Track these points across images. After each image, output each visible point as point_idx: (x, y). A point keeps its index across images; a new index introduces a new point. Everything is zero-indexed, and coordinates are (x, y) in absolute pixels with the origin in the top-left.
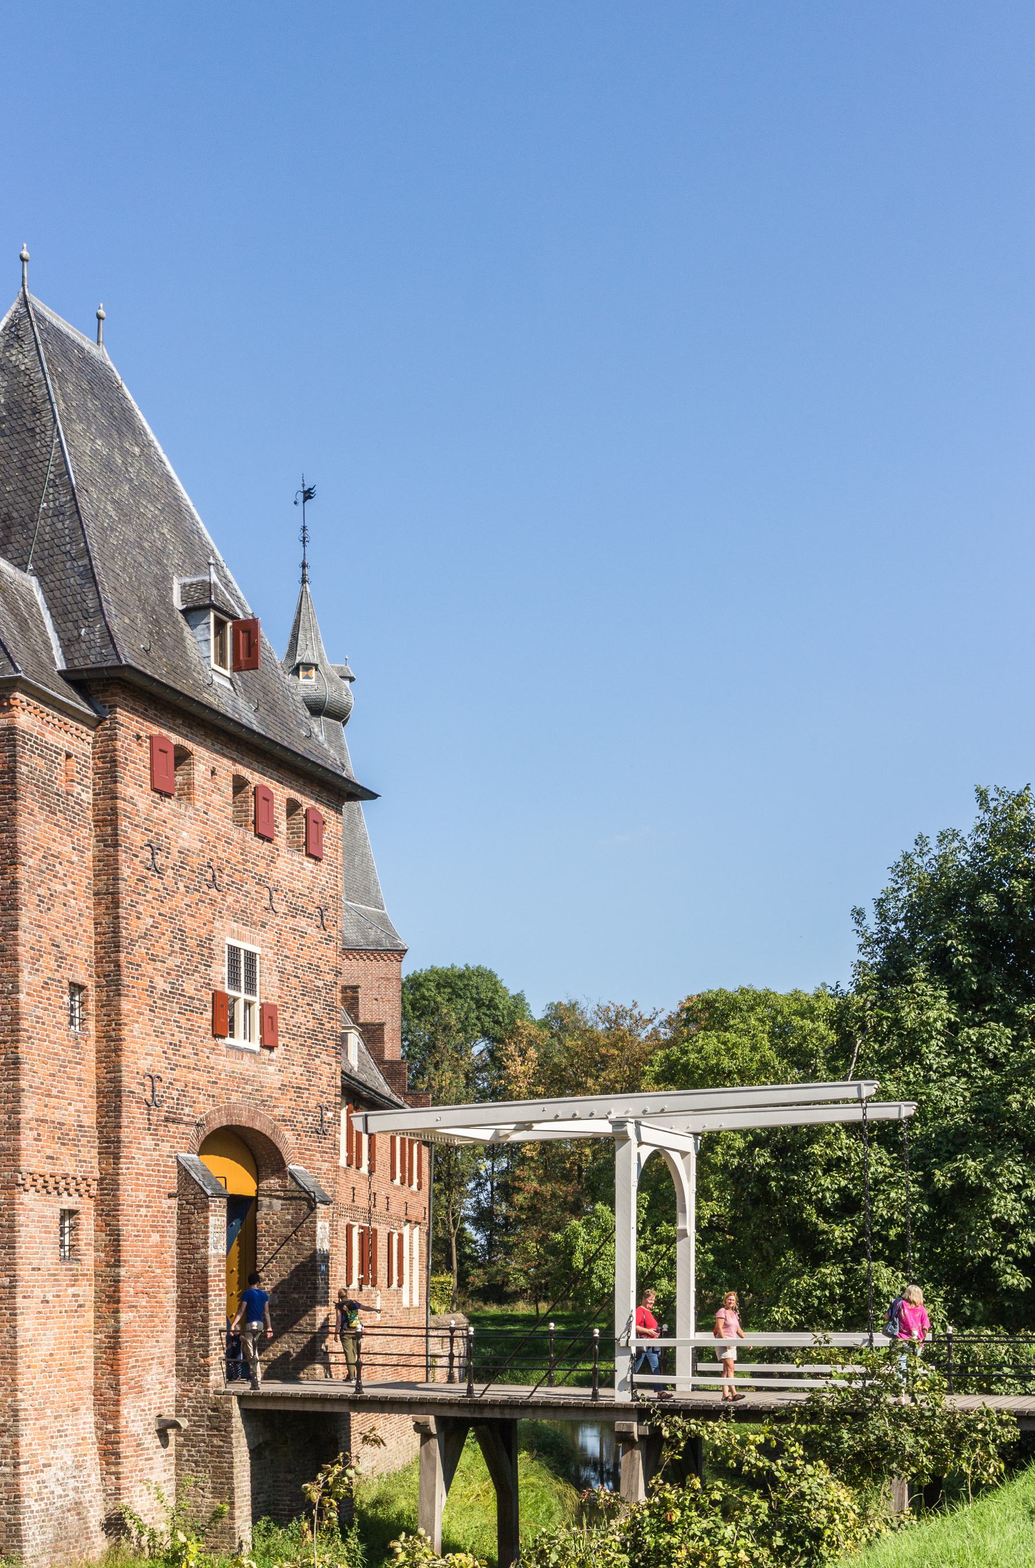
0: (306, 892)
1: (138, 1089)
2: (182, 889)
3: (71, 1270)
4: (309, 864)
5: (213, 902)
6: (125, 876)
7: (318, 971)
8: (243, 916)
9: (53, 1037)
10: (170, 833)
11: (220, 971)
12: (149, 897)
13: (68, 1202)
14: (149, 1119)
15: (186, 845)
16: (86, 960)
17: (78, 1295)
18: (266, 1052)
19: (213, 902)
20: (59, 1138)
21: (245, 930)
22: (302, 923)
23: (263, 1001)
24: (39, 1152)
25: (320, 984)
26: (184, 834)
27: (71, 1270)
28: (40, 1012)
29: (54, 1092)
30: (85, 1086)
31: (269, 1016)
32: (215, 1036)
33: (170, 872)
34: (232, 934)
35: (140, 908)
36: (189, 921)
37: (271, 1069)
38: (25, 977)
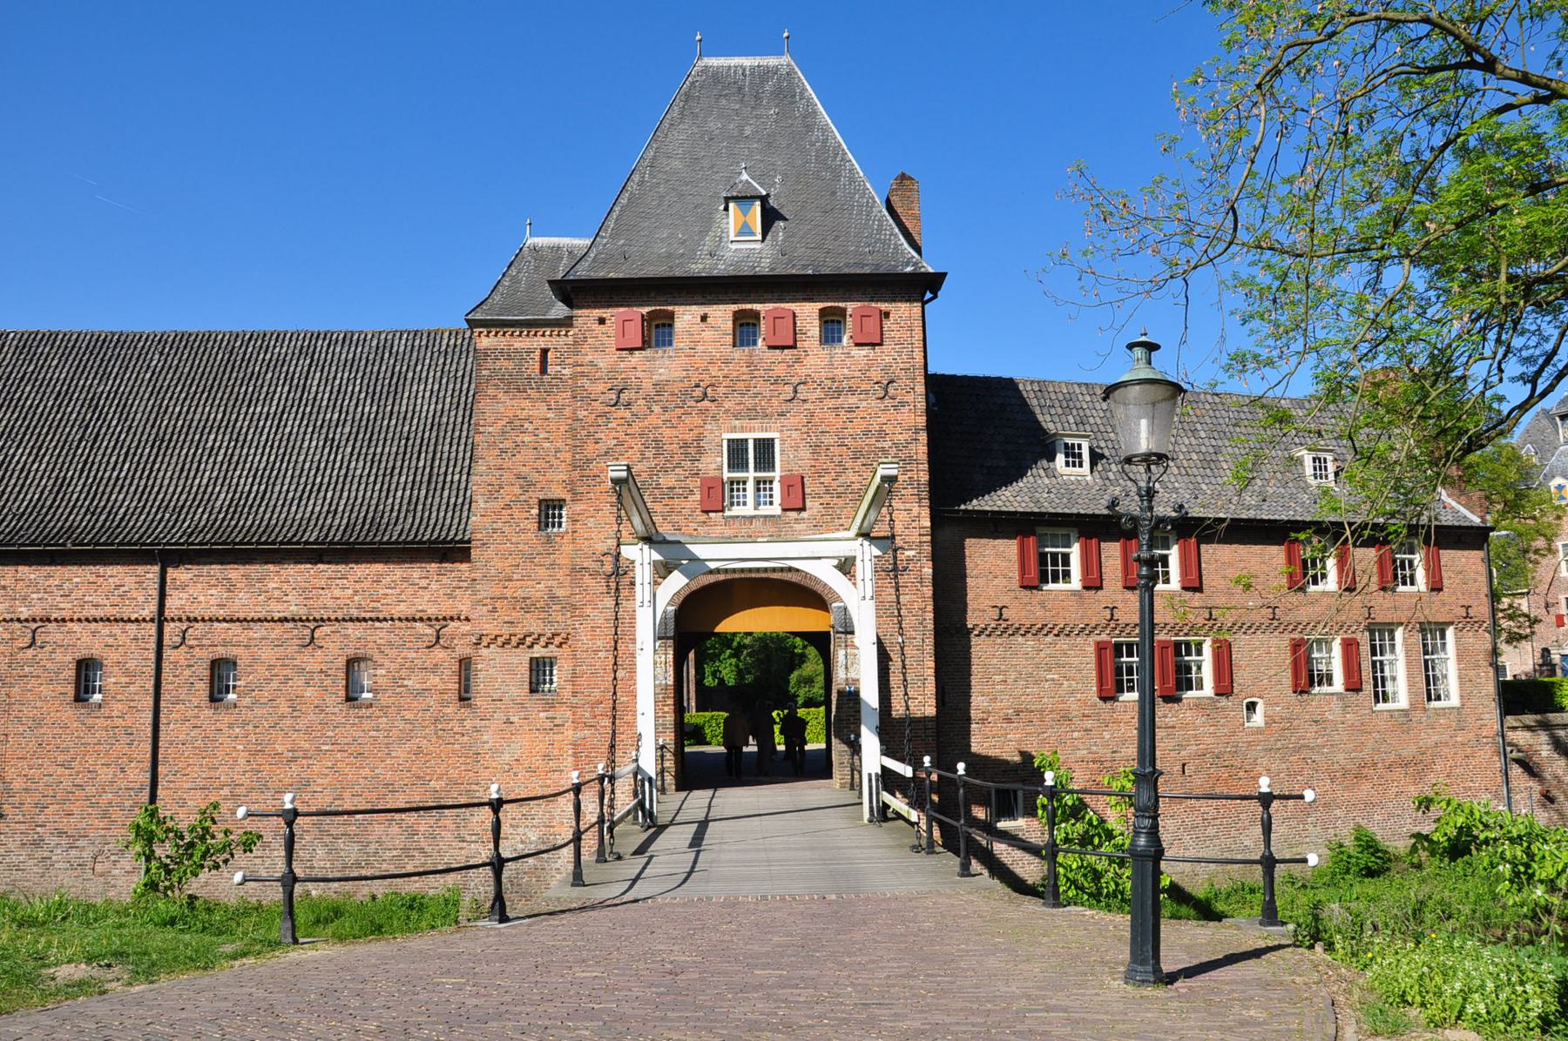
0: (858, 374)
1: (594, 566)
4: (864, 351)
5: (701, 412)
7: (882, 434)
8: (753, 414)
9: (514, 540)
10: (639, 374)
11: (717, 463)
13: (538, 651)
15: (663, 378)
18: (793, 515)
19: (701, 412)
21: (756, 424)
22: (853, 400)
25: (886, 445)
26: (661, 371)
29: (515, 577)
31: (789, 485)
32: (707, 512)
34: (733, 429)
35: (602, 436)
36: (667, 432)
37: (797, 526)
38: (480, 503)
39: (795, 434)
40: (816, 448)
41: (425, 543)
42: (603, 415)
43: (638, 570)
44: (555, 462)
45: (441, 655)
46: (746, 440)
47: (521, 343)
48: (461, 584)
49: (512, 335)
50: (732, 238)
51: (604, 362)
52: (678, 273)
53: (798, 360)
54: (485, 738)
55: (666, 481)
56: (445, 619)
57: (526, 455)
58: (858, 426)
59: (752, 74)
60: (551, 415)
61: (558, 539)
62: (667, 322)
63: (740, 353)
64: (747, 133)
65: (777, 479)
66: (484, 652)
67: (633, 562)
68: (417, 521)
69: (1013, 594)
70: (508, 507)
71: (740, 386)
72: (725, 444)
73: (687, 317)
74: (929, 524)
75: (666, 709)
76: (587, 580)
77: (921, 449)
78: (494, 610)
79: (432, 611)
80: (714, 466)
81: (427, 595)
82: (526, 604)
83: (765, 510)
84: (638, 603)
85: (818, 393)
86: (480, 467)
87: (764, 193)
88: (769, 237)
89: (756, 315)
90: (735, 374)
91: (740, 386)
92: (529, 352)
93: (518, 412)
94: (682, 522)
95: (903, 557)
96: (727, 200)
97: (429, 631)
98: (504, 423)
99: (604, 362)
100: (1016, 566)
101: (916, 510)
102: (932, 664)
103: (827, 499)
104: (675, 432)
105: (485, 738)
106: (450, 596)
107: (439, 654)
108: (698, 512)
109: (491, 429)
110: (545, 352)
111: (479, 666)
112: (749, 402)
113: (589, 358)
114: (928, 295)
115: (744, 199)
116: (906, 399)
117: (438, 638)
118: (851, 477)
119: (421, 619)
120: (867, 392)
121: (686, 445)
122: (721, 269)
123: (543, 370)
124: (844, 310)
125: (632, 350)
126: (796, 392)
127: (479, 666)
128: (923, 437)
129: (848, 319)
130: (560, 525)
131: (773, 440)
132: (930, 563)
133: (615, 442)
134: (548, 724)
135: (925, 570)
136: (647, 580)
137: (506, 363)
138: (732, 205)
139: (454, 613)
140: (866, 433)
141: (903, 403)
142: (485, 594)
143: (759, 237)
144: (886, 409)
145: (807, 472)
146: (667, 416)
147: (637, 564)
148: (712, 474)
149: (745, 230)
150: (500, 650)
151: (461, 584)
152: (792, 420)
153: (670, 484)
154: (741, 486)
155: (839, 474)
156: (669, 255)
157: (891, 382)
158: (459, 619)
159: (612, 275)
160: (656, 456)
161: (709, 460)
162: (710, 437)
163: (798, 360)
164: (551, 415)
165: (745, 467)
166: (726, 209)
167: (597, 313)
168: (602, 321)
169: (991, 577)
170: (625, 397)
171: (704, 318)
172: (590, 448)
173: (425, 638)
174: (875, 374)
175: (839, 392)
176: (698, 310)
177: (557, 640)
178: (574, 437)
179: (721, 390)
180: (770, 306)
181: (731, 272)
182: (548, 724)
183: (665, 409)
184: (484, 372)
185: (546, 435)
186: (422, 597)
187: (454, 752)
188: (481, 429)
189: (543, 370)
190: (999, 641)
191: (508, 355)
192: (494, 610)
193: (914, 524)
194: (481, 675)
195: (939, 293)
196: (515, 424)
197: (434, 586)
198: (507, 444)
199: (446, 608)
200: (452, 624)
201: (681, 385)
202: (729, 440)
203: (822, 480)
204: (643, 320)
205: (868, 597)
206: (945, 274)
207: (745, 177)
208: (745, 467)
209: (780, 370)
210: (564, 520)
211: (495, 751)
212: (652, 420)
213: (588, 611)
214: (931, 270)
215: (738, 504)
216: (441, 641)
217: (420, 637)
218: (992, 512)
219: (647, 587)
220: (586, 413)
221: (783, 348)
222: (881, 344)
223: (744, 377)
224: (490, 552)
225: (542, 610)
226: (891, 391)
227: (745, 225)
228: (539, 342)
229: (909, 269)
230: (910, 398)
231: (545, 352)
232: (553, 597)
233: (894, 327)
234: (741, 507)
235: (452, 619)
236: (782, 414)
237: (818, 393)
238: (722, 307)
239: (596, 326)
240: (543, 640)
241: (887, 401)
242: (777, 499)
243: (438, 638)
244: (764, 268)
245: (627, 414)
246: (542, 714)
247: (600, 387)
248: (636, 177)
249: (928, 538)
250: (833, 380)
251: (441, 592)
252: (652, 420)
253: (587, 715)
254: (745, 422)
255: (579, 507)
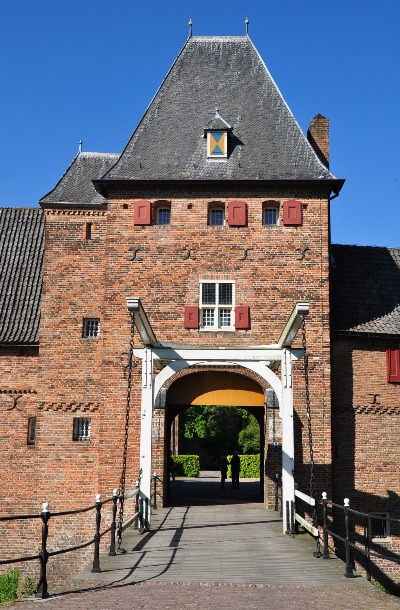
0: (286, 244)
2: (159, 263)
3: (81, 445)
4: (290, 230)
6: (111, 267)
7: (300, 282)
8: (219, 268)
10: (149, 241)
12: (129, 273)
13: (79, 414)
14: (124, 374)
15: (163, 243)
16: (99, 307)
17: (88, 457)
18: (243, 332)
20: (69, 386)
21: (220, 274)
22: (282, 260)
23: (237, 306)
24: (52, 393)
25: (303, 289)
26: (162, 239)
27: (81, 445)
28: (58, 333)
29: (67, 366)
30: (95, 362)
32: (188, 329)
33: (149, 259)
34: (206, 277)
35: (124, 279)
36: (165, 278)
37: (245, 339)
38: (46, 320)
39: (245, 281)
40: (258, 290)
41: (9, 343)
42: (125, 266)
43: (144, 363)
44: (94, 295)
45: (17, 415)
46: (214, 284)
47: (75, 219)
48: (32, 370)
49: (69, 214)
50: (209, 155)
51: (126, 233)
52: (174, 177)
53: (248, 235)
54: (43, 469)
55: (164, 308)
56: (20, 392)
57: (75, 289)
58: (285, 277)
59: (224, 48)
60: (92, 265)
61: (94, 343)
62: (166, 208)
63: (212, 229)
64: (220, 87)
65: (233, 309)
66: (45, 414)
67: (141, 359)
68: (5, 329)
69: (383, 387)
70: (63, 322)
71: (212, 250)
72: (201, 286)
73: (180, 206)
74: (329, 340)
75: (159, 453)
76: (112, 370)
77: (325, 293)
78: (52, 387)
79: (12, 386)
80: (193, 300)
81: (9, 377)
82: (73, 385)
83: (225, 328)
84: (143, 386)
85: (261, 256)
86: (46, 297)
87: (230, 127)
88: (232, 156)
89: (223, 205)
90: (208, 242)
91: (212, 250)
92: (80, 225)
93: (72, 263)
94: (173, 335)
95: (312, 361)
96: (206, 131)
97: (10, 399)
98: (62, 269)
99: (126, 233)
100: (386, 368)
101: (321, 331)
102: (329, 430)
103: (264, 322)
104: (170, 278)
105: (43, 469)
106: (24, 377)
107: (16, 414)
108: (183, 329)
109: (54, 273)
110: (89, 225)
111: (41, 423)
112: (217, 260)
113: (118, 230)
114: (333, 194)
115: (217, 131)
116: (316, 260)
117: (15, 404)
118: (279, 309)
119: (5, 392)
120: (291, 255)
121: (176, 286)
122: (201, 175)
123: (88, 237)
124: (278, 203)
125: (144, 226)
126: (246, 254)
127: (41, 423)
128: (326, 285)
129: (281, 209)
130: (96, 334)
131: (231, 284)
132: (329, 365)
133: (132, 283)
134: (84, 461)
135: (326, 369)
136: (149, 371)
137: (65, 232)
138: (209, 135)
139: (26, 388)
140: (290, 281)
141: (314, 263)
142: (46, 377)
143: (226, 156)
144: (303, 267)
145: (252, 305)
146: (165, 268)
147: (143, 361)
148: (192, 305)
149: (217, 151)
150: (55, 413)
151: (32, 370)
152: (243, 272)
153: (166, 311)
154: (210, 313)
155: (272, 307)
156: (169, 166)
157: (307, 249)
158: (29, 392)
159: (132, 178)
160: (158, 292)
161: (191, 296)
162: (193, 281)
163: (248, 235)
164: (92, 265)
165: (213, 301)
166: (205, 137)
167: (123, 201)
168: (126, 207)
169: (368, 375)
170: (139, 255)
171: (190, 207)
172: (116, 287)
173: (7, 404)
174: (297, 244)
175: (273, 256)
176: (186, 201)
177: (92, 407)
178: (106, 279)
179: (200, 252)
180: (231, 200)
181: (208, 177)
182: (84, 461)
183: (164, 263)
184: (50, 237)
185: (89, 278)
186: (6, 377)
187: (22, 478)
188: (48, 273)
189: (88, 237)
190: (373, 417)
191: (66, 226)
192: (52, 387)
193: (319, 340)
194: (42, 429)
195: (340, 193)
196: (70, 270)
197: (14, 371)
198: (64, 283)
199: (22, 385)
200: (25, 395)
201: (174, 248)
202: (203, 284)
203: (261, 310)
204: (151, 207)
205: (288, 386)
206: (344, 181)
207: (218, 116)
208: (213, 301)
209: (237, 241)
210: (98, 331)
211: (49, 478)
212: (156, 270)
213: (112, 389)
214: (335, 178)
215: (208, 324)
216: (18, 406)
217: (4, 403)
218: (370, 333)
219: (149, 376)
220: (114, 264)
221: (239, 226)
222: (301, 225)
223: (214, 244)
224: (51, 351)
225: (83, 387)
226: (307, 255)
227: (217, 147)
228: (86, 219)
229: (320, 177)
230: (319, 260)
231: (89, 225)
232: (90, 380)
233: (310, 214)
234: (210, 326)
235: (25, 392)
236: (237, 268)
237: (261, 256)
238: (201, 200)
239: (121, 209)
240: (82, 407)
241: (304, 261)
242: (233, 322)
243: (15, 404)
244: (228, 175)
245: (140, 266)
246: (80, 455)
247: (124, 248)
248: (149, 116)
249: (328, 349)
250: (270, 247)
251: (19, 375)
252: (156, 270)
253: (109, 456)
254: (214, 273)
255: (108, 324)
